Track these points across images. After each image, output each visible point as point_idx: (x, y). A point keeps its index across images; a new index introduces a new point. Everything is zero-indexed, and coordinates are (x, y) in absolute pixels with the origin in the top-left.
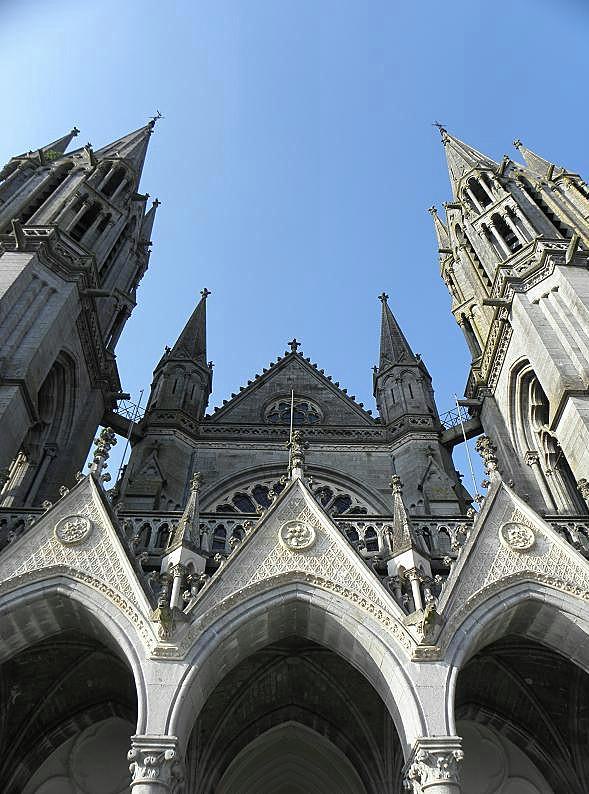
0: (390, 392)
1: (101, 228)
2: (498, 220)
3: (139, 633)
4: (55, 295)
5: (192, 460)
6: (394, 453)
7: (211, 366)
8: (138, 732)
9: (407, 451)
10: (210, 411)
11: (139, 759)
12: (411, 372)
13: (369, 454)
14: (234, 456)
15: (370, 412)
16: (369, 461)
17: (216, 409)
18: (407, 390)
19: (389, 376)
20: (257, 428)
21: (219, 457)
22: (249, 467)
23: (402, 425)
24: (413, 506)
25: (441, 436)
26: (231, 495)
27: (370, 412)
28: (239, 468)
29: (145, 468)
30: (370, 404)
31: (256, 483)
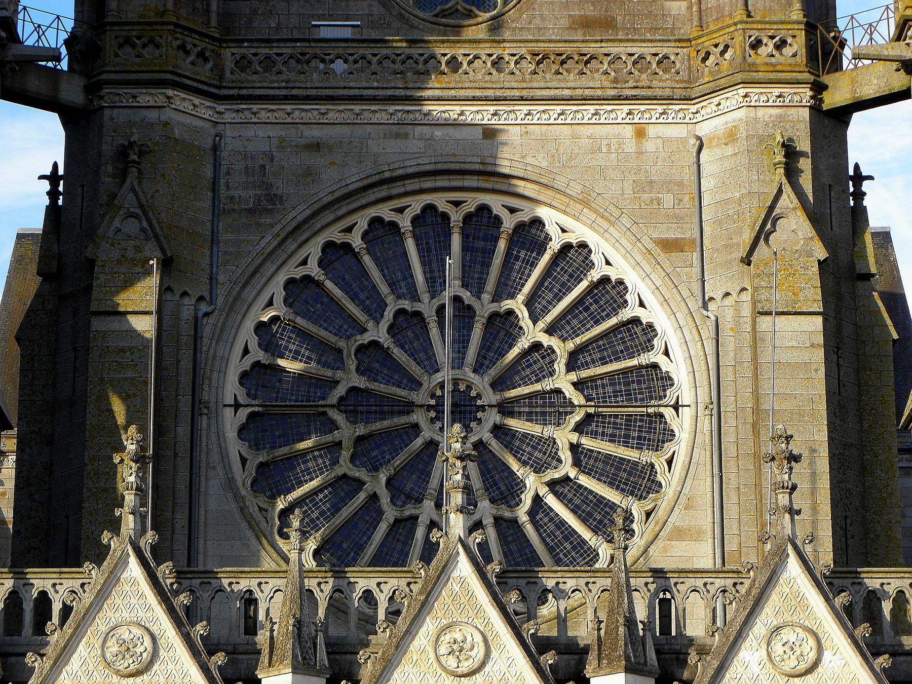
5: (216, 165)
6: (703, 130)
9: (731, 136)
13: (640, 133)
16: (640, 153)
20: (367, 52)
21: (281, 147)
22: (354, 177)
24: (727, 294)
25: (819, 88)
26: (314, 250)
28: (325, 190)
29: (117, 223)
31: (372, 212)
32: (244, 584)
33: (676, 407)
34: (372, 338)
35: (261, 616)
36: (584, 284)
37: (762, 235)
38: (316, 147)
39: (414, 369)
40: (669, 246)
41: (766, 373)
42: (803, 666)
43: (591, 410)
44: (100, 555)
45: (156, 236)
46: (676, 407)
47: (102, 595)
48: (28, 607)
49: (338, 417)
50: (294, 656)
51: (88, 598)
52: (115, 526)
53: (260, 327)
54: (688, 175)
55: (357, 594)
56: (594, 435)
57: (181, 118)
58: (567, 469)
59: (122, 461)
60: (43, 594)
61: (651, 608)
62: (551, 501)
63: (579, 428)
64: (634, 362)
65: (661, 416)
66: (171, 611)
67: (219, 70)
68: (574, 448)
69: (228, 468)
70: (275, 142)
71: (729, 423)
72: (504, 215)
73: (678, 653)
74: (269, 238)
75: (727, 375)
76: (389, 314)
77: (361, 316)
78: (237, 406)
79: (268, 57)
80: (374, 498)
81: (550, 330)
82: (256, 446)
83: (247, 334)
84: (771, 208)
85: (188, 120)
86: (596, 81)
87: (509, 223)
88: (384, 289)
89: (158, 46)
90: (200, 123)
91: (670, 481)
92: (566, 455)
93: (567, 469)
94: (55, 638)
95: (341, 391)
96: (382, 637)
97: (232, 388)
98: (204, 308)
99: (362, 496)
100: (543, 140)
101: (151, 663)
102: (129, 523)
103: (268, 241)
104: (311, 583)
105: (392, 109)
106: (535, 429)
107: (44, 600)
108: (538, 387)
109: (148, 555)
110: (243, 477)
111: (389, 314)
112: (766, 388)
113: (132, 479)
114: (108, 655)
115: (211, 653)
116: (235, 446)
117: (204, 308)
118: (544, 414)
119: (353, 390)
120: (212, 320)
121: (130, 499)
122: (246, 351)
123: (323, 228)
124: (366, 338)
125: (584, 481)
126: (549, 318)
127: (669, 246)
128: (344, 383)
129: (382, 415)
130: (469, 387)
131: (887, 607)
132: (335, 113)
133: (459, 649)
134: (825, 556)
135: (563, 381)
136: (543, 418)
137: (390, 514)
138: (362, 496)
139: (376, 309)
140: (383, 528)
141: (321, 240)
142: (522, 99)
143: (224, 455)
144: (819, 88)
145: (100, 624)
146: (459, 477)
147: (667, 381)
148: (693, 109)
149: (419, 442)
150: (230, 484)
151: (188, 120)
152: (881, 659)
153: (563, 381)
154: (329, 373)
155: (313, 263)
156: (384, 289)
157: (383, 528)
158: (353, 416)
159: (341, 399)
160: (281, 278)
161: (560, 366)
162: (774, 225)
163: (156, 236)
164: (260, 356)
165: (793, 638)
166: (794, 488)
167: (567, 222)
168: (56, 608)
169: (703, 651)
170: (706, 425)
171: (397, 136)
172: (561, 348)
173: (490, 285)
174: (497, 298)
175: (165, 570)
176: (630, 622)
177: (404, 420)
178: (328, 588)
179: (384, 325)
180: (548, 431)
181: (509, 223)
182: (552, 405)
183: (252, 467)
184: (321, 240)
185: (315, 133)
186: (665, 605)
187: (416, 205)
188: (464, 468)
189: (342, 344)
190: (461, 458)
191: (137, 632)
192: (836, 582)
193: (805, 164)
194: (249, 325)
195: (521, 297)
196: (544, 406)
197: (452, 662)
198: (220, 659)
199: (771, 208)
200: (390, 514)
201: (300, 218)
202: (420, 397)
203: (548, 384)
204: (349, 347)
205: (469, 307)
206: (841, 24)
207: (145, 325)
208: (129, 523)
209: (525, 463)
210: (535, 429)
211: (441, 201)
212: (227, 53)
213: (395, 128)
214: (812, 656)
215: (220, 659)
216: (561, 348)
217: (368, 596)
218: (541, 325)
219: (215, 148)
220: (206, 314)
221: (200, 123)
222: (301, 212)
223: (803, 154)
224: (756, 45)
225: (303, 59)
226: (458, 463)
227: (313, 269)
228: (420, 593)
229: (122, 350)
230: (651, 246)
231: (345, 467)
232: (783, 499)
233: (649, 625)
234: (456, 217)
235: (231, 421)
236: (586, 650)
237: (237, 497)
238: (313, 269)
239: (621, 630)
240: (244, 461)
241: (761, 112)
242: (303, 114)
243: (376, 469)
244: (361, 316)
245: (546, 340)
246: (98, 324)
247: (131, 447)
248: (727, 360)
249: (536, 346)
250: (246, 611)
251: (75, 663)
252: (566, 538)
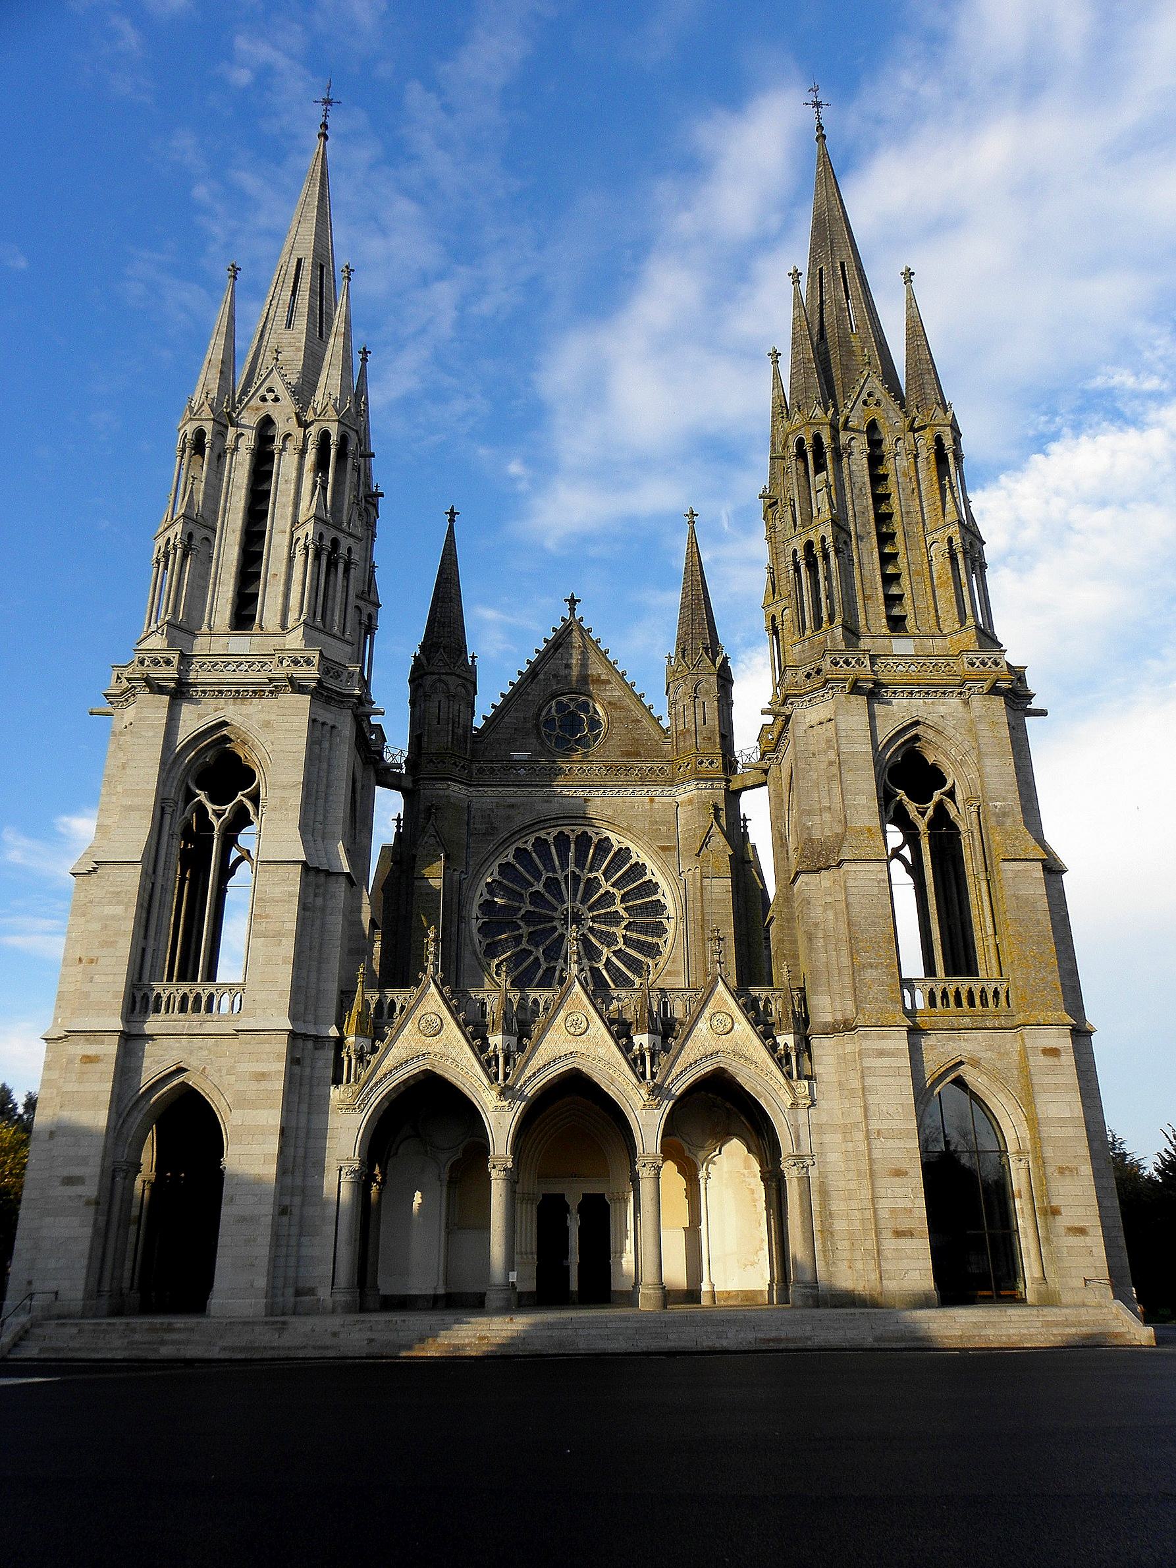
0: (682, 710)
1: (347, 571)
2: (809, 545)
3: (483, 1095)
4: (335, 732)
5: (469, 814)
6: (679, 799)
7: (473, 657)
8: (491, 1153)
9: (691, 801)
10: (478, 723)
11: (494, 1167)
12: (707, 681)
13: (652, 801)
15: (660, 718)
17: (485, 718)
18: (699, 711)
19: (680, 685)
22: (528, 820)
23: (688, 764)
24: (690, 869)
25: (728, 781)
26: (511, 851)
27: (660, 718)
28: (518, 823)
30: (661, 709)
31: (537, 835)
32: (480, 996)
33: (668, 918)
35: (488, 1010)
36: (628, 865)
37: (704, 844)
38: (512, 806)
39: (555, 902)
40: (664, 849)
41: (707, 904)
42: (726, 1030)
43: (632, 920)
44: (417, 983)
45: (443, 845)
46: (668, 918)
47: (419, 1001)
48: (386, 1007)
49: (521, 924)
50: (503, 1027)
51: (412, 1002)
52: (424, 970)
53: (488, 884)
54: (672, 818)
55: (530, 1001)
56: (633, 931)
57: (452, 793)
58: (621, 945)
59: (428, 942)
60: (392, 1001)
61: (659, 1005)
62: (614, 959)
63: (626, 928)
64: (650, 899)
65: (661, 922)
66: (449, 1008)
67: (470, 772)
68: (624, 936)
69: (473, 946)
70: (494, 804)
71: (691, 925)
72: (593, 835)
73: (671, 1025)
75: (690, 905)
76: (543, 878)
77: (532, 880)
78: (477, 918)
79: (492, 768)
80: (537, 959)
81: (613, 885)
82: (485, 936)
83: (482, 888)
84: (708, 832)
85: (457, 795)
86: (632, 779)
87: (595, 840)
88: (541, 868)
89: (444, 763)
90: (462, 796)
91: (665, 950)
92: (621, 940)
93: (621, 945)
94: (397, 1020)
95: (522, 912)
96: (542, 1018)
97: (475, 911)
98: (463, 876)
99: (532, 958)
100: (610, 804)
101: (440, 1031)
102: (431, 968)
103: (491, 847)
104: (510, 995)
106: (607, 928)
107: (393, 1003)
108: (608, 910)
109: (439, 983)
110: (480, 950)
111: (543, 878)
112: (707, 910)
113: (432, 949)
114: (421, 1028)
115: (466, 1026)
116: (477, 937)
117: (463, 876)
118: (610, 922)
120: (467, 881)
121: (431, 958)
122: (481, 895)
123: (515, 841)
124: (534, 889)
125: (628, 950)
126: (613, 880)
127: (664, 849)
129: (541, 923)
130: (578, 911)
131: (761, 1004)
132: (520, 791)
133: (575, 1024)
134: (733, 981)
135: (619, 907)
136: (611, 924)
137: (544, 966)
138: (532, 958)
140: (541, 971)
141: (514, 846)
142: (601, 785)
143: (472, 940)
144: (728, 781)
145: (418, 1013)
146: (575, 948)
147: (664, 907)
148: (675, 790)
149: (557, 934)
150: (475, 952)
151: (457, 795)
152: (759, 1027)
153: (619, 907)
154: (518, 904)
155: (511, 856)
156: (541, 868)
157: (541, 971)
158: (528, 923)
159: (522, 915)
160: (497, 863)
161: (618, 901)
162: (709, 839)
163: (443, 845)
164: (488, 897)
165: (721, 1018)
166: (721, 951)
167: (621, 839)
168: (398, 1007)
169: (682, 1024)
170: (681, 926)
171: (547, 802)
172: (618, 894)
173: (587, 867)
174: (590, 871)
175: (446, 989)
176: (650, 1012)
177: (550, 924)
178: (517, 998)
179: (541, 884)
180: (613, 929)
181: (595, 840)
182: (614, 918)
183: (484, 945)
185: (512, 800)
186: (665, 1003)
187: (555, 832)
188: (577, 944)
189: (523, 891)
190: (576, 940)
191: (434, 1017)
192: (739, 993)
193: (722, 814)
194: (483, 883)
195: (600, 871)
196: (611, 918)
197: (572, 1030)
198: (470, 1028)
199: (708, 832)
200: (544, 966)
202: (556, 915)
203: (613, 909)
204: (527, 894)
205: (579, 876)
206: (737, 754)
207: (437, 883)
208: (431, 968)
209: (603, 943)
210: (607, 928)
211: (566, 830)
212: (474, 766)
214: (730, 1026)
215: (470, 1028)
216: (618, 894)
217: (535, 1002)
218: (609, 883)
219: (469, 806)
220: (464, 879)
221: (462, 796)
222: (506, 835)
223: (722, 809)
224: (701, 763)
225: (506, 769)
226: (575, 942)
227: (511, 859)
228: (559, 999)
229: (428, 894)
230: (657, 849)
231: (524, 945)
232: (716, 957)
233: (658, 1013)
234: (572, 837)
235: (475, 925)
236: (631, 1024)
237: (477, 958)
238: (511, 859)
239: (646, 1015)
240: (480, 942)
241: (703, 791)
243: (537, 946)
244: (532, 880)
245: (611, 890)
246: (417, 883)
247: (432, 935)
248: (690, 898)
249: (607, 892)
250: (482, 1008)
251: (406, 1031)
252: (643, 945)
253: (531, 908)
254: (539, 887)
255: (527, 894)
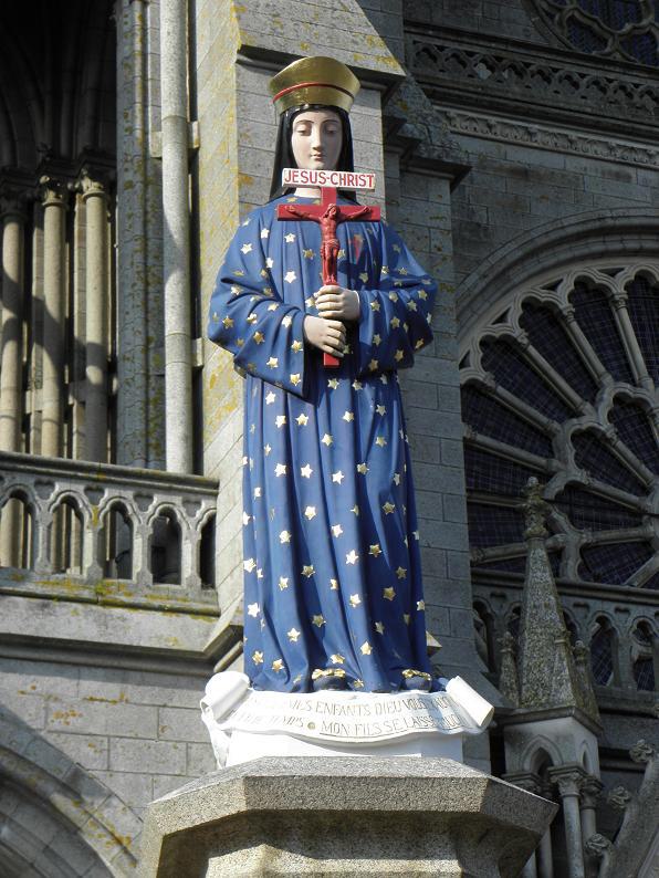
14: (523, 174)
31: (578, 270)
34: (590, 424)
74: (474, 277)
105: (614, 142)
119: (572, 487)
124: (585, 423)
128: (562, 474)
139: (591, 390)
171: (618, 176)
177: (634, 532)
184: (520, 295)
187: (630, 269)
201: (510, 259)
213: (615, 168)
222: (511, 252)
242: (507, 131)
253: (581, 476)
254: (597, 417)
255: (565, 431)
